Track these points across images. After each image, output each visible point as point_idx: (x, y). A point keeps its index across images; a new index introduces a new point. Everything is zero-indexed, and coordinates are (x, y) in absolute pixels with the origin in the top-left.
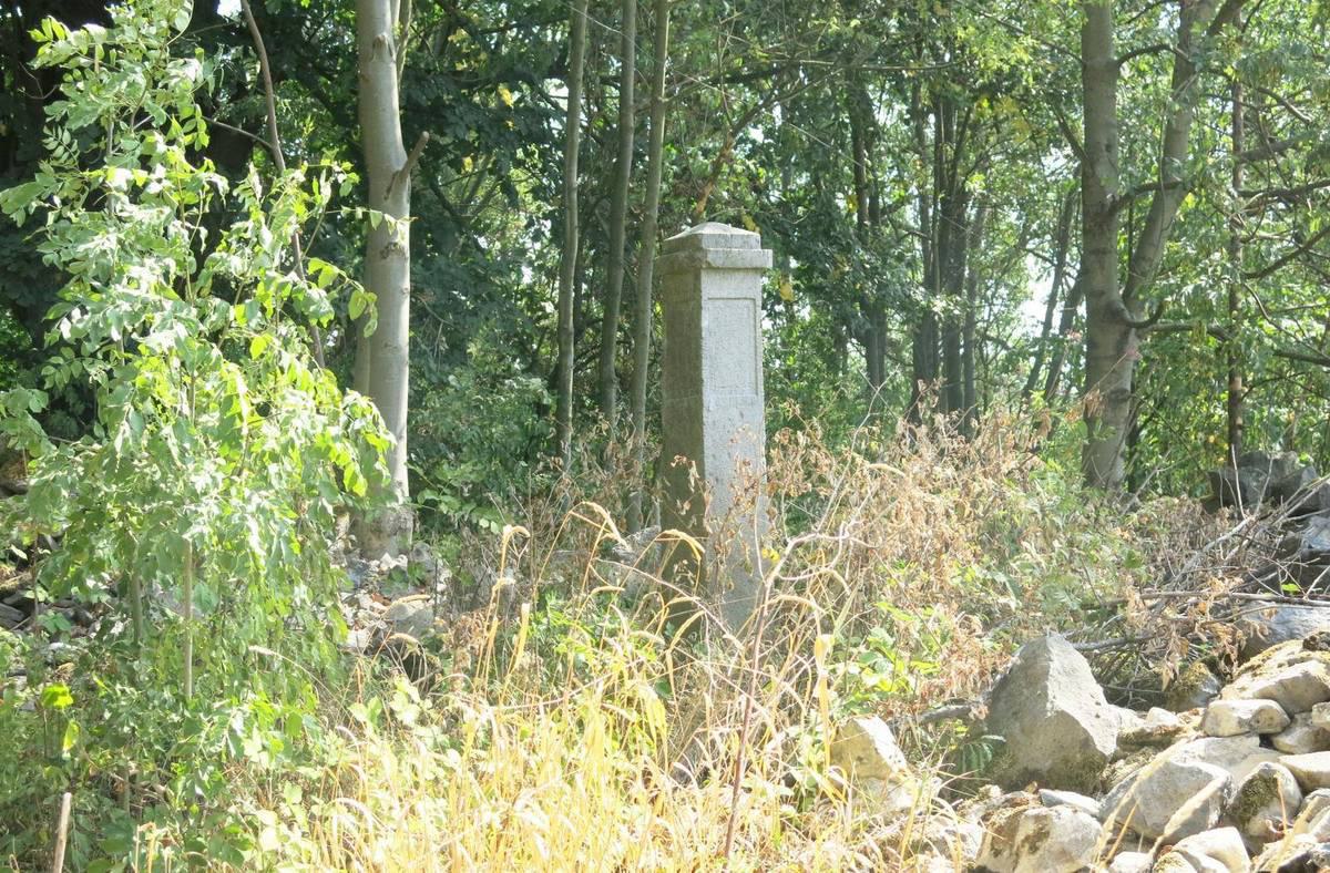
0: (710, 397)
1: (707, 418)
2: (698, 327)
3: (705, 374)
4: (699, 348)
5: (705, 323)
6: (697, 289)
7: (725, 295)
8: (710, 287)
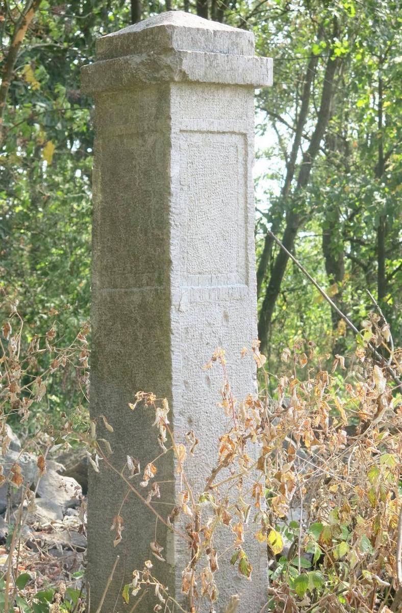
0: (181, 288)
1: (178, 321)
2: (165, 177)
3: (175, 252)
4: (163, 210)
5: (175, 171)
6: (162, 113)
7: (204, 126)
8: (186, 113)
